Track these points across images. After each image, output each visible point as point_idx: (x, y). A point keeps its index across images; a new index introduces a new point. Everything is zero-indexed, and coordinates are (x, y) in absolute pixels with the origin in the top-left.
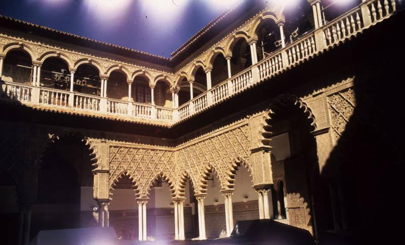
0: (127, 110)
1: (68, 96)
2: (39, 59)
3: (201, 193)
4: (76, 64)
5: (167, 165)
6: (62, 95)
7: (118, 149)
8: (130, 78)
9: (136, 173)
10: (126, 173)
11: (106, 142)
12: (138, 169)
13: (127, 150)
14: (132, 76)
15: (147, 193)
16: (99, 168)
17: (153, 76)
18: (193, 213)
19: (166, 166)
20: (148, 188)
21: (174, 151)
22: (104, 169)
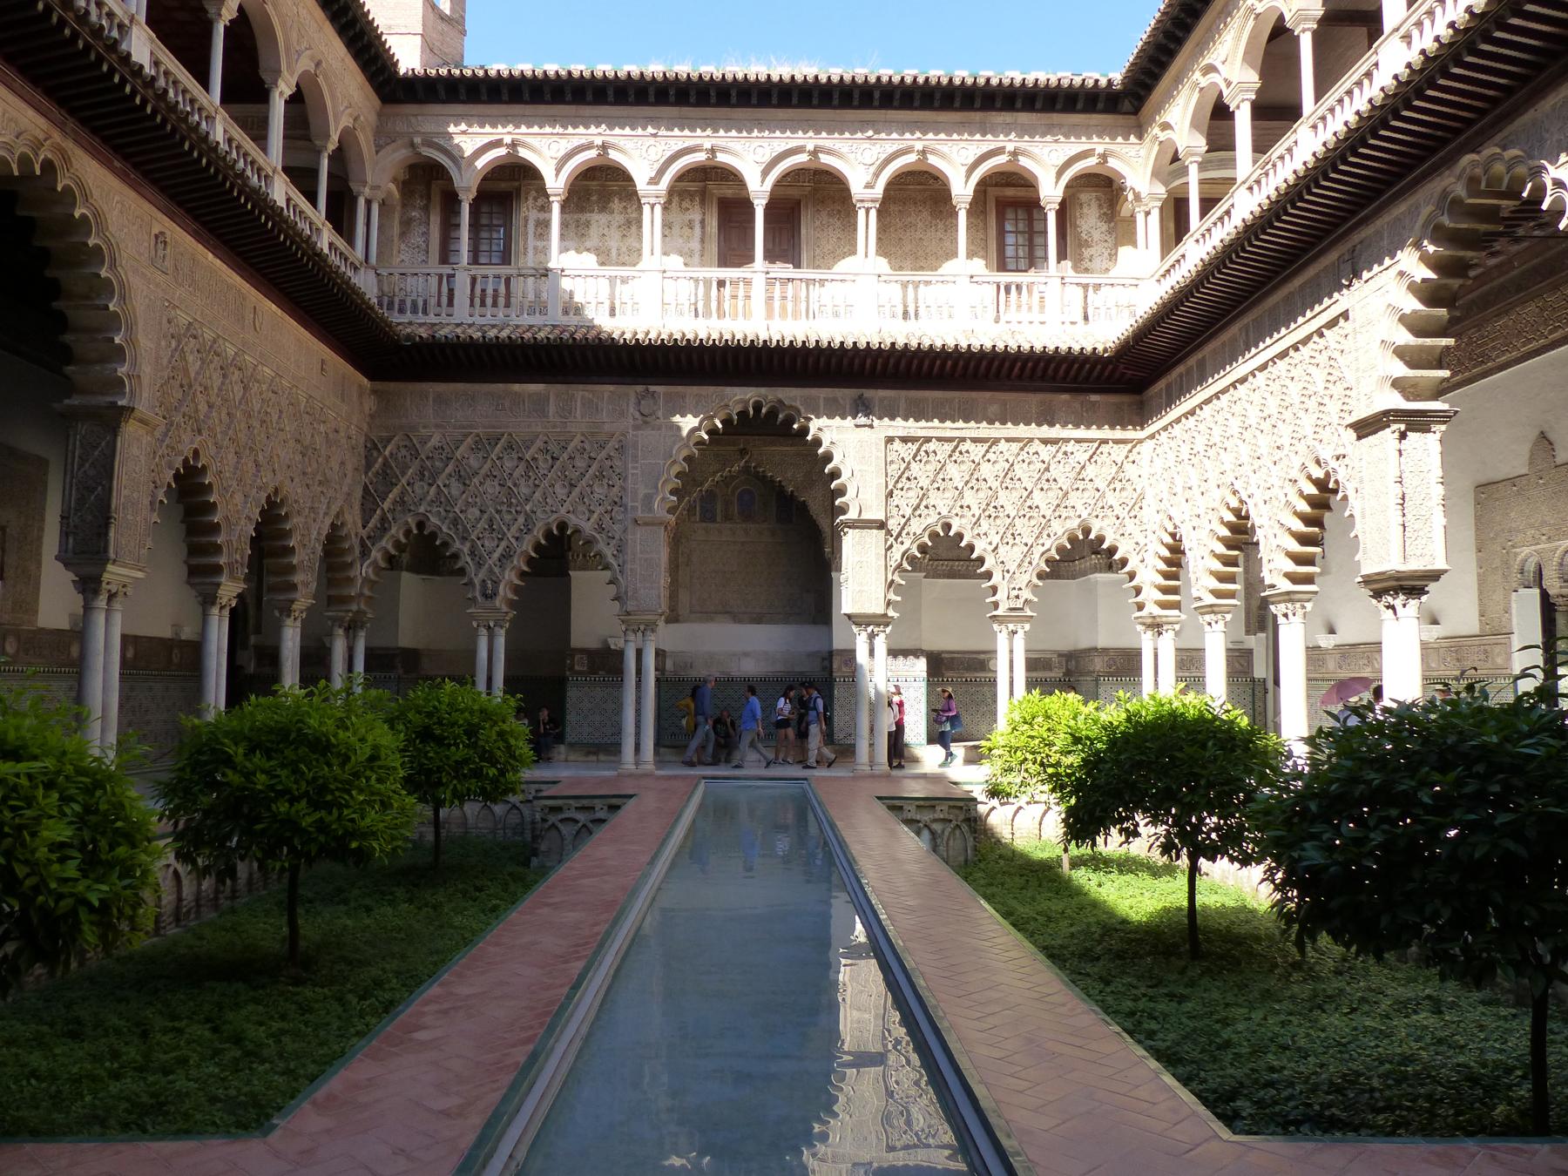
0: (961, 304)
1: (748, 282)
2: (654, 181)
3: (1210, 600)
4: (765, 173)
7: (917, 445)
8: (962, 190)
9: (984, 523)
11: (871, 426)
12: (992, 509)
13: (949, 447)
14: (968, 176)
15: (1027, 594)
16: (852, 514)
17: (1049, 159)
18: (1260, 671)
20: (1029, 576)
21: (1141, 441)
22: (865, 516)
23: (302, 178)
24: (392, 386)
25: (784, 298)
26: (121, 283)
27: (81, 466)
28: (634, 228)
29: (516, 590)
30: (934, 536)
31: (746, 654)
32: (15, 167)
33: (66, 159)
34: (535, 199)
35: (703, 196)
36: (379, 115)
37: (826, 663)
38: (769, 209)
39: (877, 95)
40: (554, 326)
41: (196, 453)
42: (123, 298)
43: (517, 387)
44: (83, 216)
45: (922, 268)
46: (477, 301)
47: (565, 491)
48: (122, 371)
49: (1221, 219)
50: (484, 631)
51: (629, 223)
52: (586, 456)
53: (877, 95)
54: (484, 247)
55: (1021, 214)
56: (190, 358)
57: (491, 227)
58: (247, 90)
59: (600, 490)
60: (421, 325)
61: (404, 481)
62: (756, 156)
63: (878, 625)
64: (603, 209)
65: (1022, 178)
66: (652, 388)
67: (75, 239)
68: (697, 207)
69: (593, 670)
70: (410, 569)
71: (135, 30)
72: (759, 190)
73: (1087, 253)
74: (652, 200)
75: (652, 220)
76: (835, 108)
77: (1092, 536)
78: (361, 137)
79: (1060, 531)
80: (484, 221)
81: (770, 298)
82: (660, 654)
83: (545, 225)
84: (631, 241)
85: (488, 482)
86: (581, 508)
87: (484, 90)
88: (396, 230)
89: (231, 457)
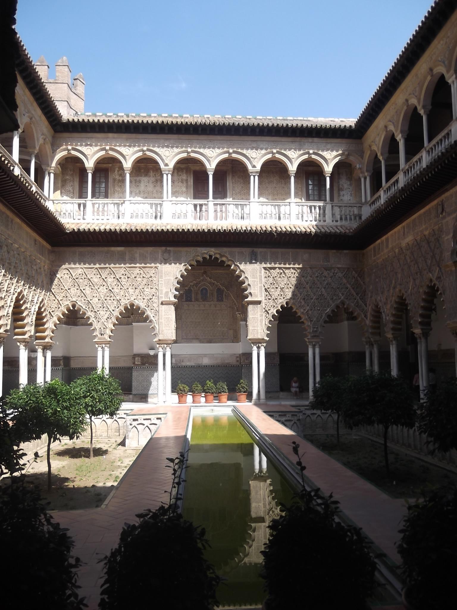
5: (352, 290)
6: (198, 206)
8: (293, 168)
16: (249, 299)
19: (350, 290)
24: (62, 249)
25: (221, 211)
28: (159, 183)
31: (205, 355)
35: (187, 170)
36: (53, 137)
37: (238, 359)
38: (214, 175)
39: (258, 130)
40: (128, 224)
43: (113, 249)
45: (276, 199)
46: (96, 213)
47: (133, 290)
49: (394, 183)
50: (100, 349)
51: (157, 181)
54: (97, 191)
57: (100, 182)
60: (73, 223)
63: (260, 343)
64: (146, 175)
65: (316, 163)
66: (168, 248)
69: (143, 364)
72: (211, 166)
73: (342, 193)
75: (167, 180)
76: (240, 135)
77: (345, 306)
79: (333, 305)
80: (97, 180)
83: (123, 181)
84: (158, 188)
85: (102, 287)
86: (139, 297)
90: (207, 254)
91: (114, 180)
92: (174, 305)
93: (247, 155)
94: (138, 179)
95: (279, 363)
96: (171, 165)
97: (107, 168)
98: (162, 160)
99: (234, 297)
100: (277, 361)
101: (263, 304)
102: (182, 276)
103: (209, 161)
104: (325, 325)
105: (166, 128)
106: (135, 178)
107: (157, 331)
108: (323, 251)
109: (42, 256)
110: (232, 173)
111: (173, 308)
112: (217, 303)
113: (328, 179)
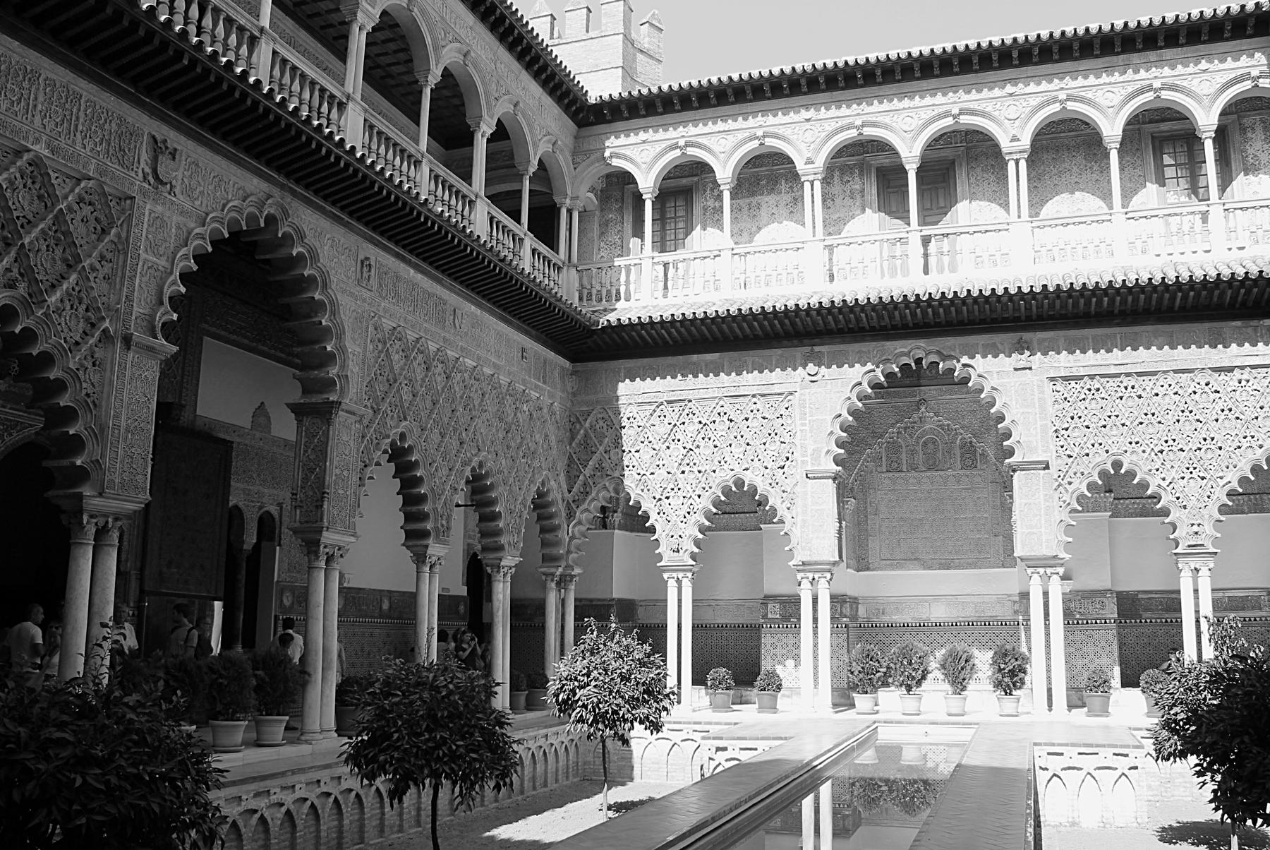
8: (1112, 130)
10: (1117, 465)
15: (1208, 529)
23: (506, 201)
24: (590, 365)
26: (332, 303)
27: (306, 451)
28: (799, 204)
29: (697, 543)
30: (1103, 474)
31: (936, 598)
32: (243, 223)
33: (285, 213)
34: (712, 190)
35: (863, 168)
38: (919, 172)
39: (1015, 54)
41: (403, 437)
42: (333, 313)
43: (695, 357)
44: (299, 253)
47: (742, 449)
48: (333, 372)
52: (759, 416)
53: (1015, 54)
55: (1182, 148)
56: (396, 357)
58: (452, 135)
59: (773, 447)
61: (601, 449)
62: (908, 124)
64: (771, 191)
66: (817, 349)
67: (298, 272)
68: (857, 179)
70: (623, 527)
71: (351, 105)
72: (910, 154)
74: (811, 178)
78: (561, 158)
81: (926, 255)
82: (836, 599)
87: (659, 104)
88: (596, 233)
89: (436, 438)
90: (907, 354)
91: (705, 209)
92: (834, 479)
93: (996, 113)
94: (755, 200)
95: (1116, 616)
96: (820, 161)
97: (686, 187)
98: (799, 151)
99: (982, 453)
100: (1111, 611)
101: (1053, 470)
102: (853, 412)
103: (903, 140)
104: (1222, 518)
105: (803, 82)
106: (748, 200)
107: (794, 540)
108: (1207, 325)
109: (545, 382)
110: (960, 161)
111: (830, 487)
112: (962, 472)
113: (1209, 146)
